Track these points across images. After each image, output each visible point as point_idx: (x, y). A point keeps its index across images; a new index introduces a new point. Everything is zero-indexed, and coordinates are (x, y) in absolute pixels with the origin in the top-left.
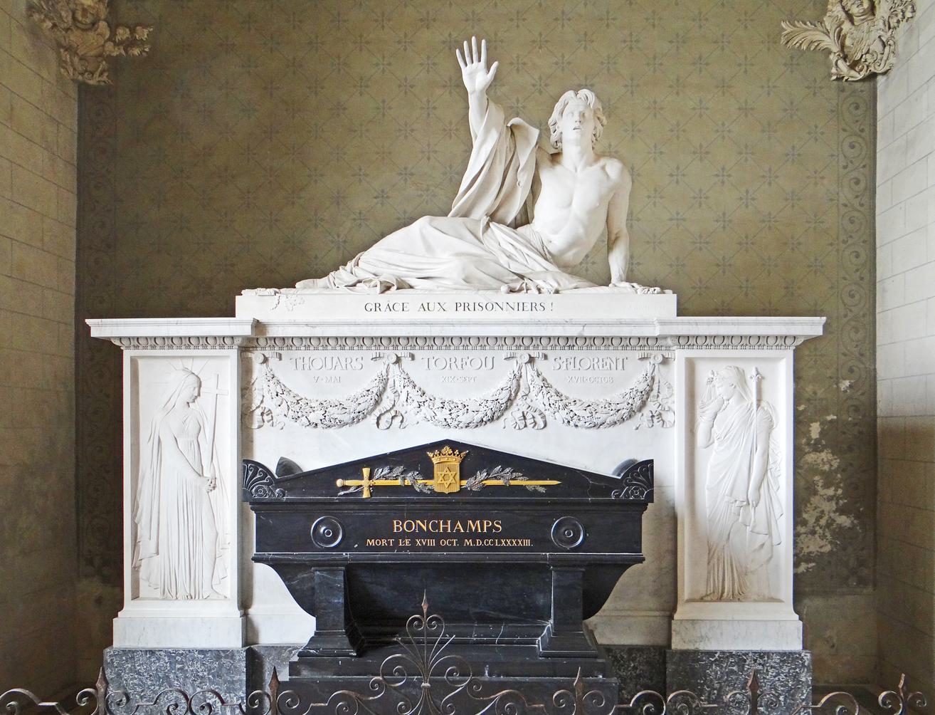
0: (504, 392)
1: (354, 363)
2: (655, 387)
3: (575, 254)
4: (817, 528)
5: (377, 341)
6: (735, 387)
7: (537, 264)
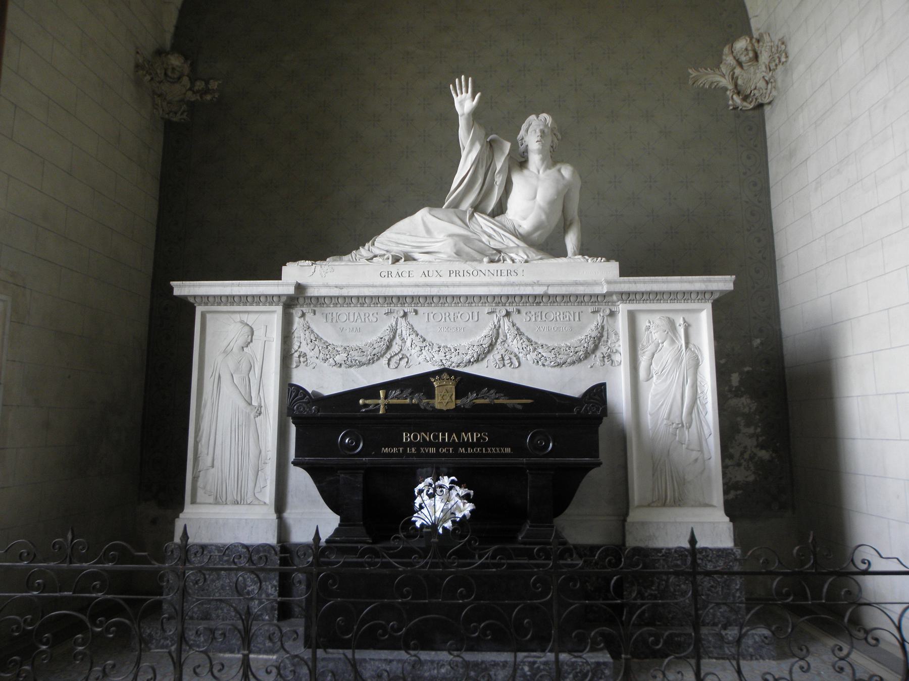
1: (371, 317)
2: (605, 334)
3: (540, 235)
4: (742, 461)
5: (388, 299)
7: (511, 241)
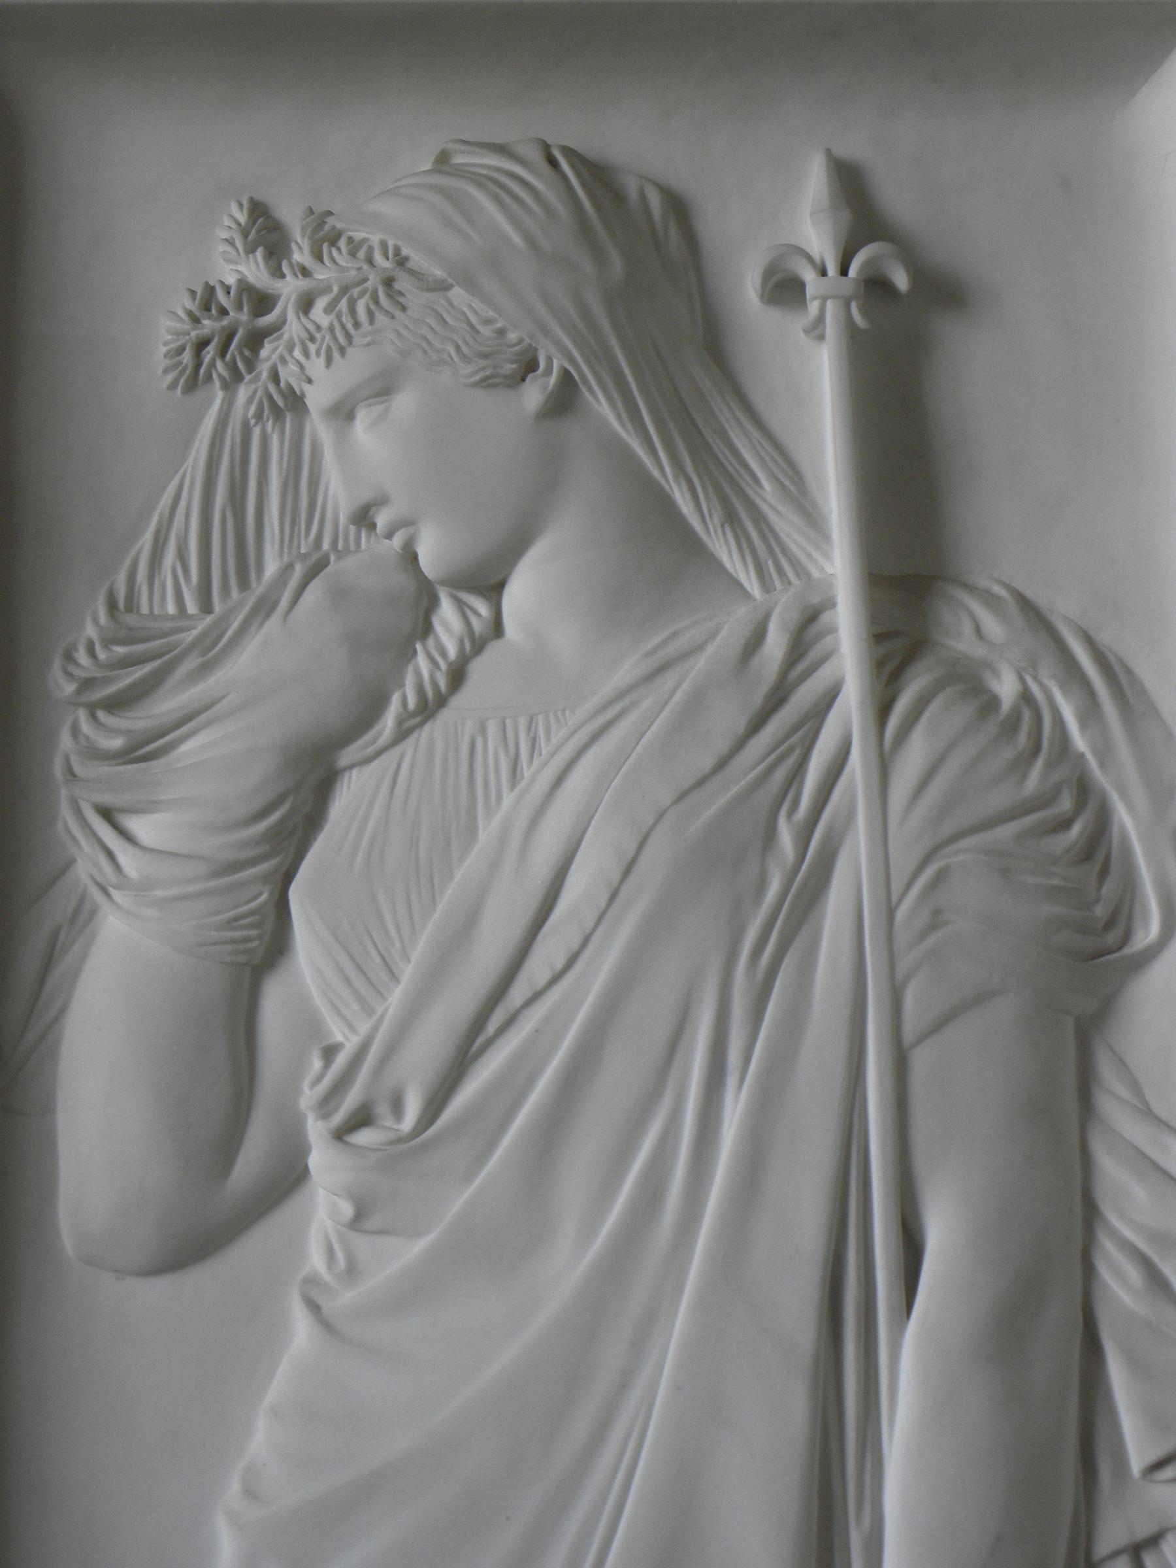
6: (564, 400)
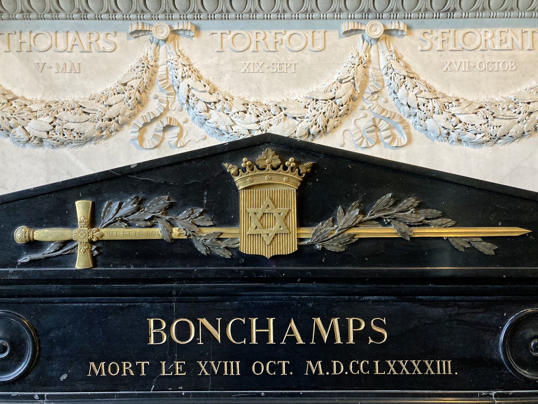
0: (343, 85)
